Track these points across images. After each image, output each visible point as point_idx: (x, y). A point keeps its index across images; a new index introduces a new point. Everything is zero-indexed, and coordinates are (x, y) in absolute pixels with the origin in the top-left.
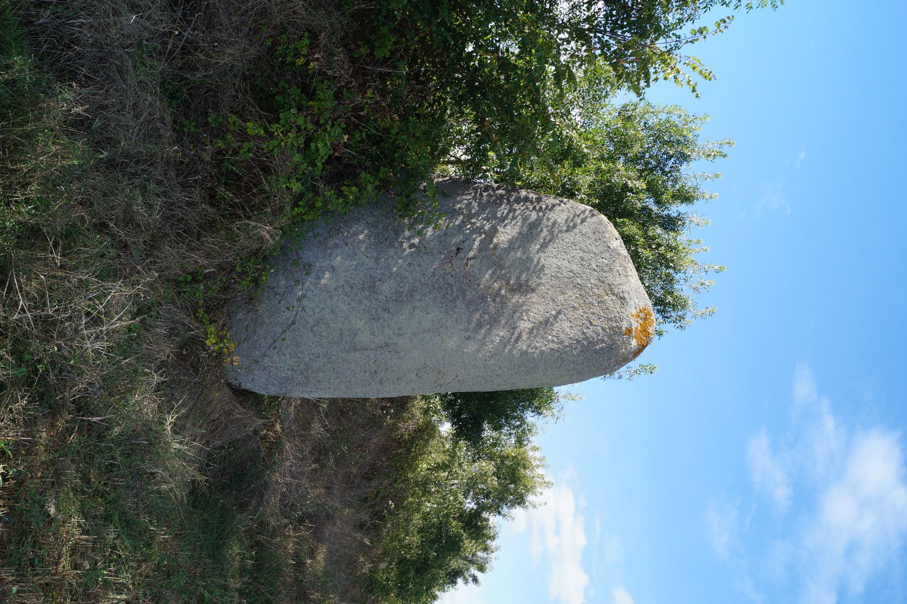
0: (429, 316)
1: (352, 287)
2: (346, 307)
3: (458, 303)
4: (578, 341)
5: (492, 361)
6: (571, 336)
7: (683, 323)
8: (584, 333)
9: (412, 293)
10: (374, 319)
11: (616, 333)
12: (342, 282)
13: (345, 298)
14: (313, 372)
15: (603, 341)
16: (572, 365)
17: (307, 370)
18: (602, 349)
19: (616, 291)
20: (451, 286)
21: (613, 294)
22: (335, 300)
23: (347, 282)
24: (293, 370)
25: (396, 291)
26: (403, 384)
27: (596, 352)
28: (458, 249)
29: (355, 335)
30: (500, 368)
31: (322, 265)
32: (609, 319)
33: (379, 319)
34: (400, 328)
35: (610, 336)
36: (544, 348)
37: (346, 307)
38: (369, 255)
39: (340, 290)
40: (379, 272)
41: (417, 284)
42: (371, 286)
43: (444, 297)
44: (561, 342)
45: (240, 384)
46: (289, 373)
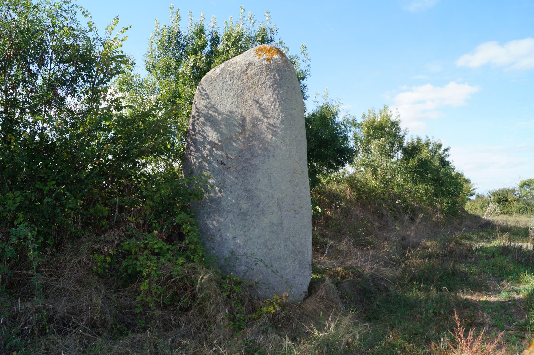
0: (261, 180)
1: (245, 226)
2: (257, 230)
3: (253, 163)
4: (275, 90)
5: (287, 141)
6: (271, 94)
7: (274, 30)
8: (270, 87)
9: (248, 191)
10: (263, 213)
11: (269, 68)
12: (242, 233)
13: (251, 230)
14: (296, 249)
15: (274, 75)
16: (289, 93)
17: (294, 252)
18: (279, 76)
19: (245, 69)
20: (243, 167)
21: (247, 70)
22: (252, 236)
23: (242, 229)
24: (294, 261)
25: (247, 200)
26: (302, 194)
27: (281, 79)
28: (222, 164)
29: (273, 224)
30: (291, 136)
31: (232, 244)
32: (261, 72)
33: (263, 210)
34: (269, 197)
35: (271, 71)
36: (279, 111)
37: (257, 230)
38: (226, 217)
39: (247, 233)
40: (235, 210)
41: (242, 188)
42: (244, 215)
43: (250, 171)
44: (275, 100)
45: (304, 292)
46: (296, 263)
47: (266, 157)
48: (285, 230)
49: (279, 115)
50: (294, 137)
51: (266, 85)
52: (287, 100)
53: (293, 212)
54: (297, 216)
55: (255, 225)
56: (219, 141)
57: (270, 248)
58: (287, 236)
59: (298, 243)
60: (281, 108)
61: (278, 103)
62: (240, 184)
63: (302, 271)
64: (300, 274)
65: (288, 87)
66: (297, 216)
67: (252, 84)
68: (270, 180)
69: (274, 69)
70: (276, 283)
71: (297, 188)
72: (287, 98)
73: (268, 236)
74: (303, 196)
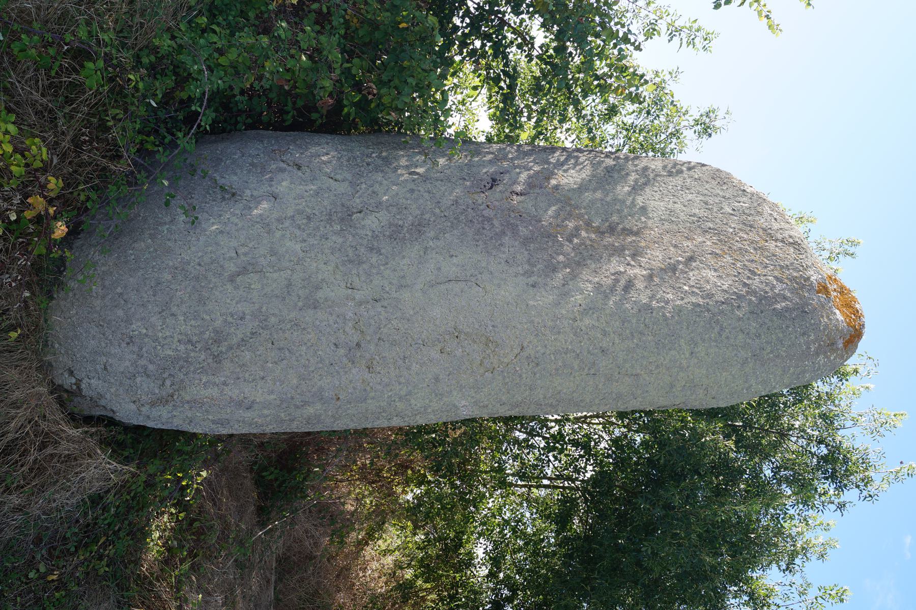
0: (455, 260)
1: (309, 218)
2: (298, 247)
3: (506, 240)
4: (739, 297)
5: (587, 321)
6: (725, 287)
7: (872, 489)
8: (745, 285)
9: (419, 227)
10: (350, 261)
11: (802, 287)
12: (290, 213)
13: (298, 232)
14: (230, 348)
15: (785, 298)
16: (741, 336)
17: (217, 342)
18: (787, 309)
19: (779, 236)
20: (489, 220)
21: (776, 240)
22: (278, 234)
23: (300, 212)
24: (190, 341)
25: (390, 225)
26: (415, 367)
27: (780, 314)
28: (494, 180)
29: (318, 288)
30: (605, 334)
31: (255, 193)
32: (782, 267)
33: (360, 263)
34: (403, 277)
35: (793, 291)
36: (678, 302)
37: (298, 247)
38: (338, 177)
39: (287, 223)
40: (358, 201)
41: (427, 216)
42: (346, 216)
43: (478, 232)
44: (710, 296)
45: (78, 382)
46: (182, 348)
47: (527, 267)
48: (293, 315)
49: (667, 302)
50: (604, 344)
51: (749, 278)
52: (717, 329)
53: (356, 338)
54: (342, 351)
55: (312, 241)
56: (556, 187)
57: (239, 279)
58: (273, 320)
59: (248, 355)
60: (690, 307)
61: (701, 301)
62: (437, 211)
63: (151, 367)
64: (142, 362)
65: (759, 336)
66: (342, 351)
67: (740, 249)
68: (457, 280)
69: (801, 297)
70: (119, 290)
71: (434, 353)
72: (722, 329)
73: (275, 275)
74: (409, 369)
